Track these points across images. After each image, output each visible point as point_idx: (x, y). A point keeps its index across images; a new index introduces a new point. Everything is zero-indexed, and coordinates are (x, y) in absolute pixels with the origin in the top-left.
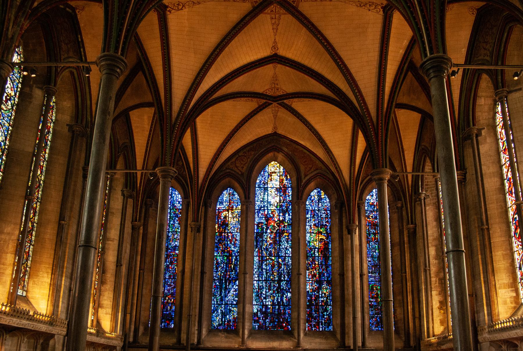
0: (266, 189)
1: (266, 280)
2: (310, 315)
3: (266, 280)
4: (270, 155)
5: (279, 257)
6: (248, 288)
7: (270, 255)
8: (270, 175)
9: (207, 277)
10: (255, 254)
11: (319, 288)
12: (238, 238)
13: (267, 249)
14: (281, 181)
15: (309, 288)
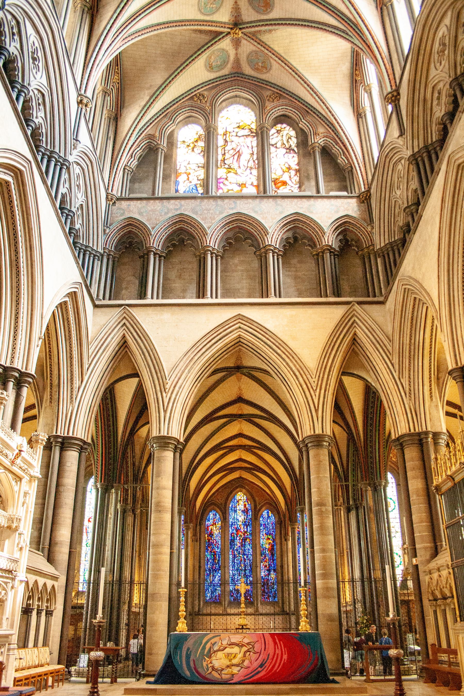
0: (235, 511)
1: (237, 570)
2: (264, 591)
3: (237, 570)
4: (238, 489)
5: (244, 554)
6: (227, 576)
7: (239, 553)
8: (238, 502)
9: (202, 570)
10: (230, 553)
11: (269, 574)
12: (220, 543)
13: (237, 550)
14: (245, 505)
15: (263, 574)
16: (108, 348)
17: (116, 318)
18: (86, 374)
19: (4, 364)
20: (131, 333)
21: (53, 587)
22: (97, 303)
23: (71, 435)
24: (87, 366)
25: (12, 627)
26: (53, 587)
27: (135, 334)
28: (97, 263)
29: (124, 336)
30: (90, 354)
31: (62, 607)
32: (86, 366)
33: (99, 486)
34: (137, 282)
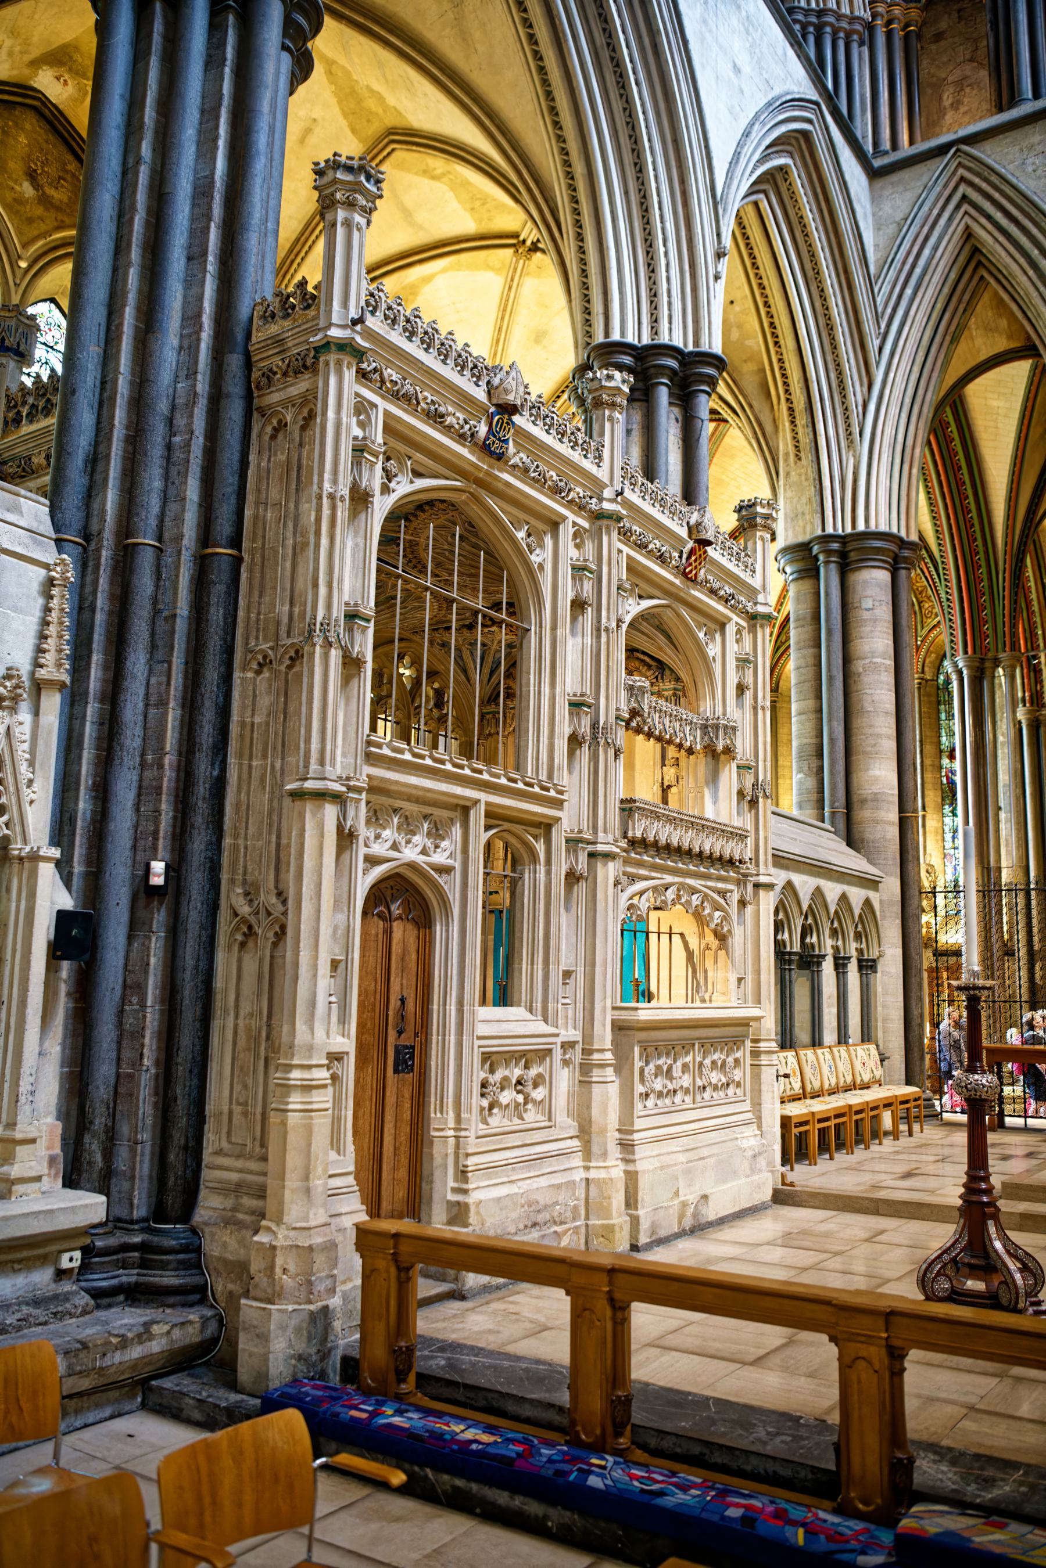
16: (927, 278)
17: (938, 189)
18: (878, 364)
19: (636, 342)
20: (989, 218)
21: (868, 903)
22: (877, 163)
23: (861, 527)
24: (877, 343)
25: (758, 1000)
26: (868, 903)
27: (998, 216)
28: (860, 55)
29: (968, 235)
30: (880, 309)
31: (899, 952)
32: (873, 343)
33: (961, 664)
34: (984, 75)
